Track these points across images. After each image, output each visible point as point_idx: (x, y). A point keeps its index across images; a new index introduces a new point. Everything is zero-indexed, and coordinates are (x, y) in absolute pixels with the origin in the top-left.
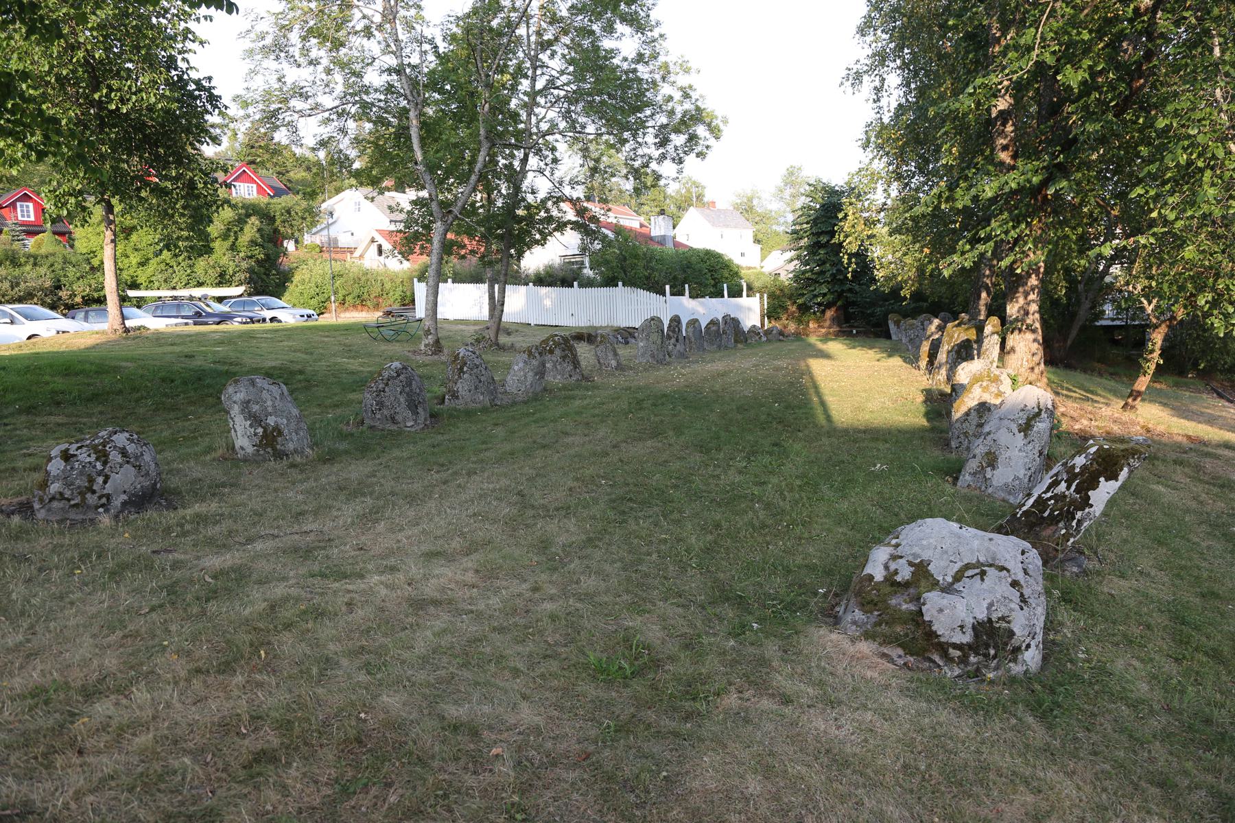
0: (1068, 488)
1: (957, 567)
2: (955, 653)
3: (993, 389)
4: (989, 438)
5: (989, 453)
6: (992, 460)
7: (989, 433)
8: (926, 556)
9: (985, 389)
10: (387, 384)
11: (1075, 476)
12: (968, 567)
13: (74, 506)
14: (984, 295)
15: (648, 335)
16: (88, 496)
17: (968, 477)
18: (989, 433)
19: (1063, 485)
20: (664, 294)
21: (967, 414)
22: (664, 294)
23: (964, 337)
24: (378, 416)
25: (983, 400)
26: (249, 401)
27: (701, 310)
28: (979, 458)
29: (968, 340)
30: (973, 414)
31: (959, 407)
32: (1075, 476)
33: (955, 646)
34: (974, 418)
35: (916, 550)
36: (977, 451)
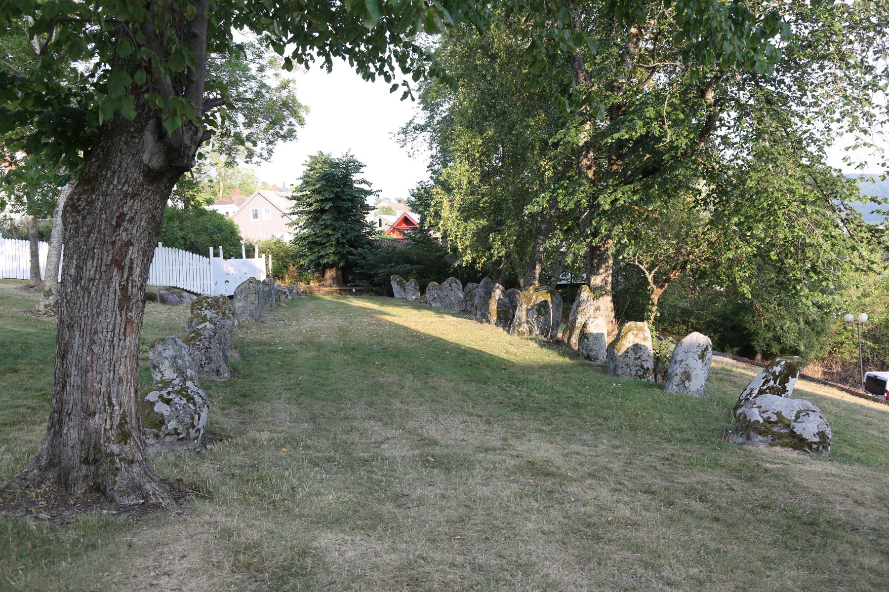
0: (775, 383)
1: (795, 413)
2: (815, 446)
3: (641, 335)
4: (683, 363)
5: (685, 372)
6: (687, 376)
7: (682, 361)
8: (779, 409)
9: (636, 336)
10: (210, 342)
11: (777, 377)
12: (799, 412)
13: (182, 439)
14: (538, 267)
15: (247, 296)
16: (191, 430)
17: (675, 387)
18: (682, 361)
19: (772, 382)
20: (208, 256)
21: (627, 352)
22: (208, 256)
23: (541, 299)
24: (205, 369)
25: (636, 342)
26: (175, 357)
27: (232, 270)
28: (679, 375)
29: (546, 301)
30: (631, 352)
31: (620, 347)
32: (777, 377)
33: (815, 443)
34: (632, 355)
35: (773, 407)
36: (677, 371)
